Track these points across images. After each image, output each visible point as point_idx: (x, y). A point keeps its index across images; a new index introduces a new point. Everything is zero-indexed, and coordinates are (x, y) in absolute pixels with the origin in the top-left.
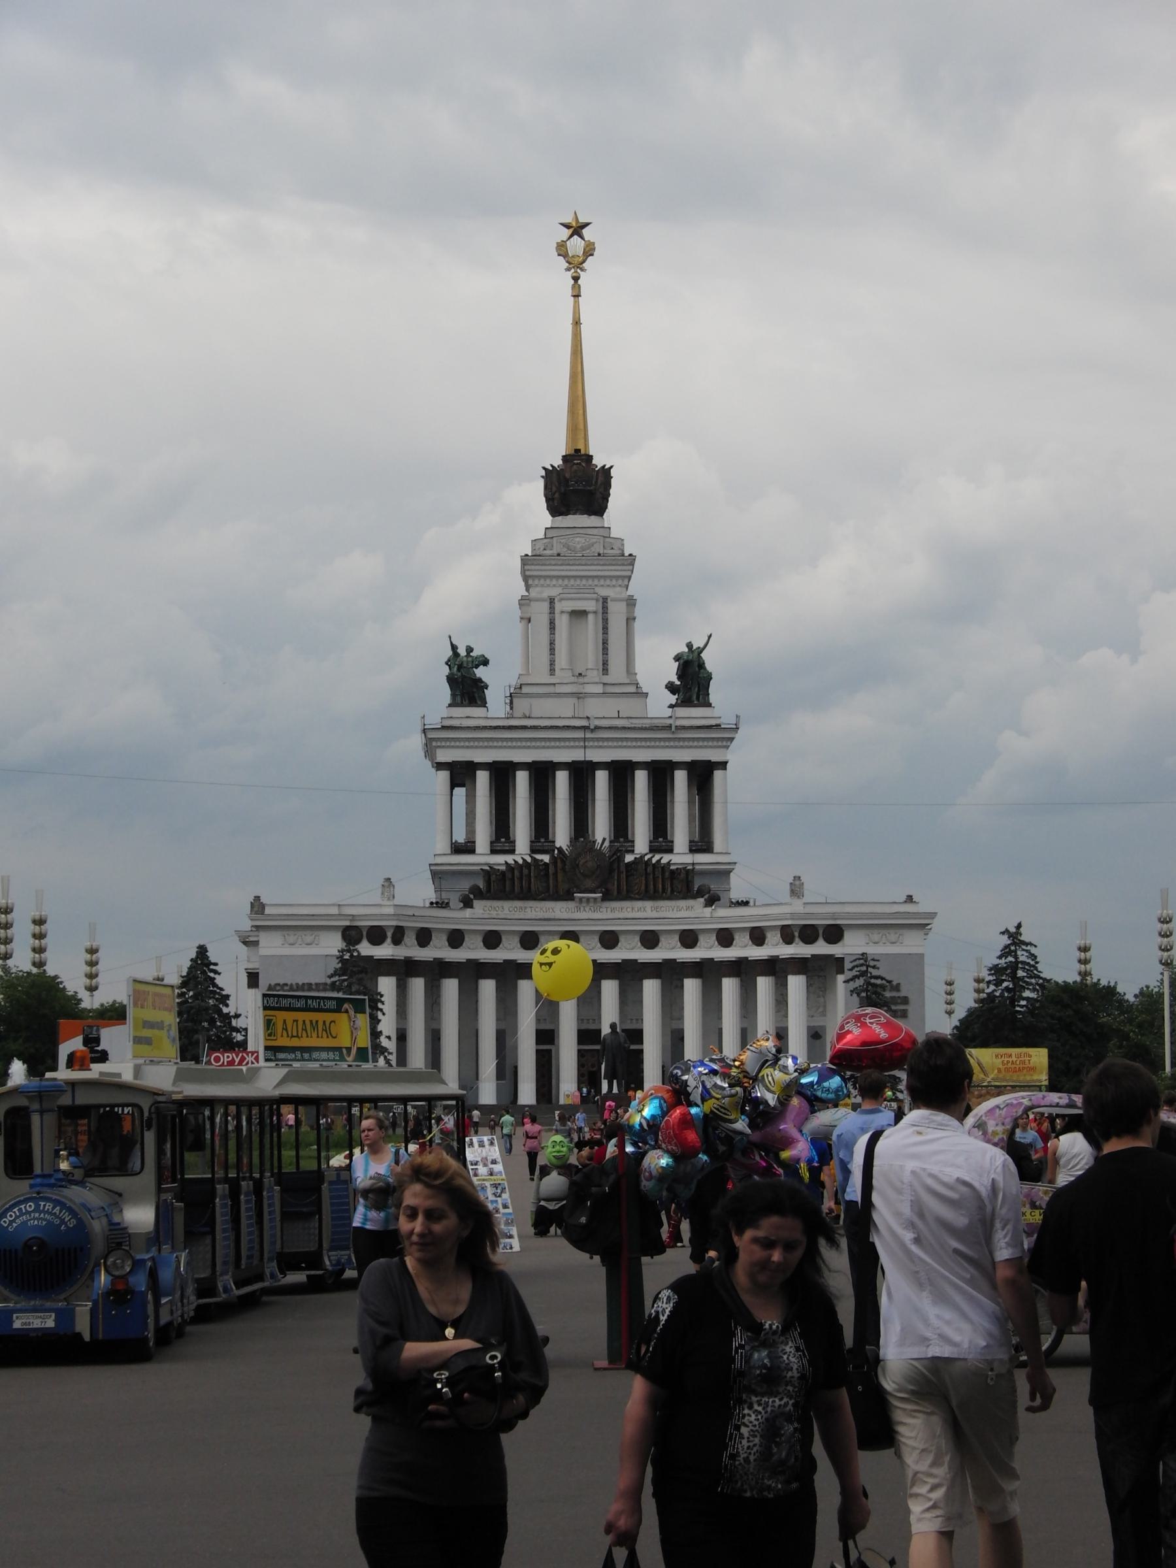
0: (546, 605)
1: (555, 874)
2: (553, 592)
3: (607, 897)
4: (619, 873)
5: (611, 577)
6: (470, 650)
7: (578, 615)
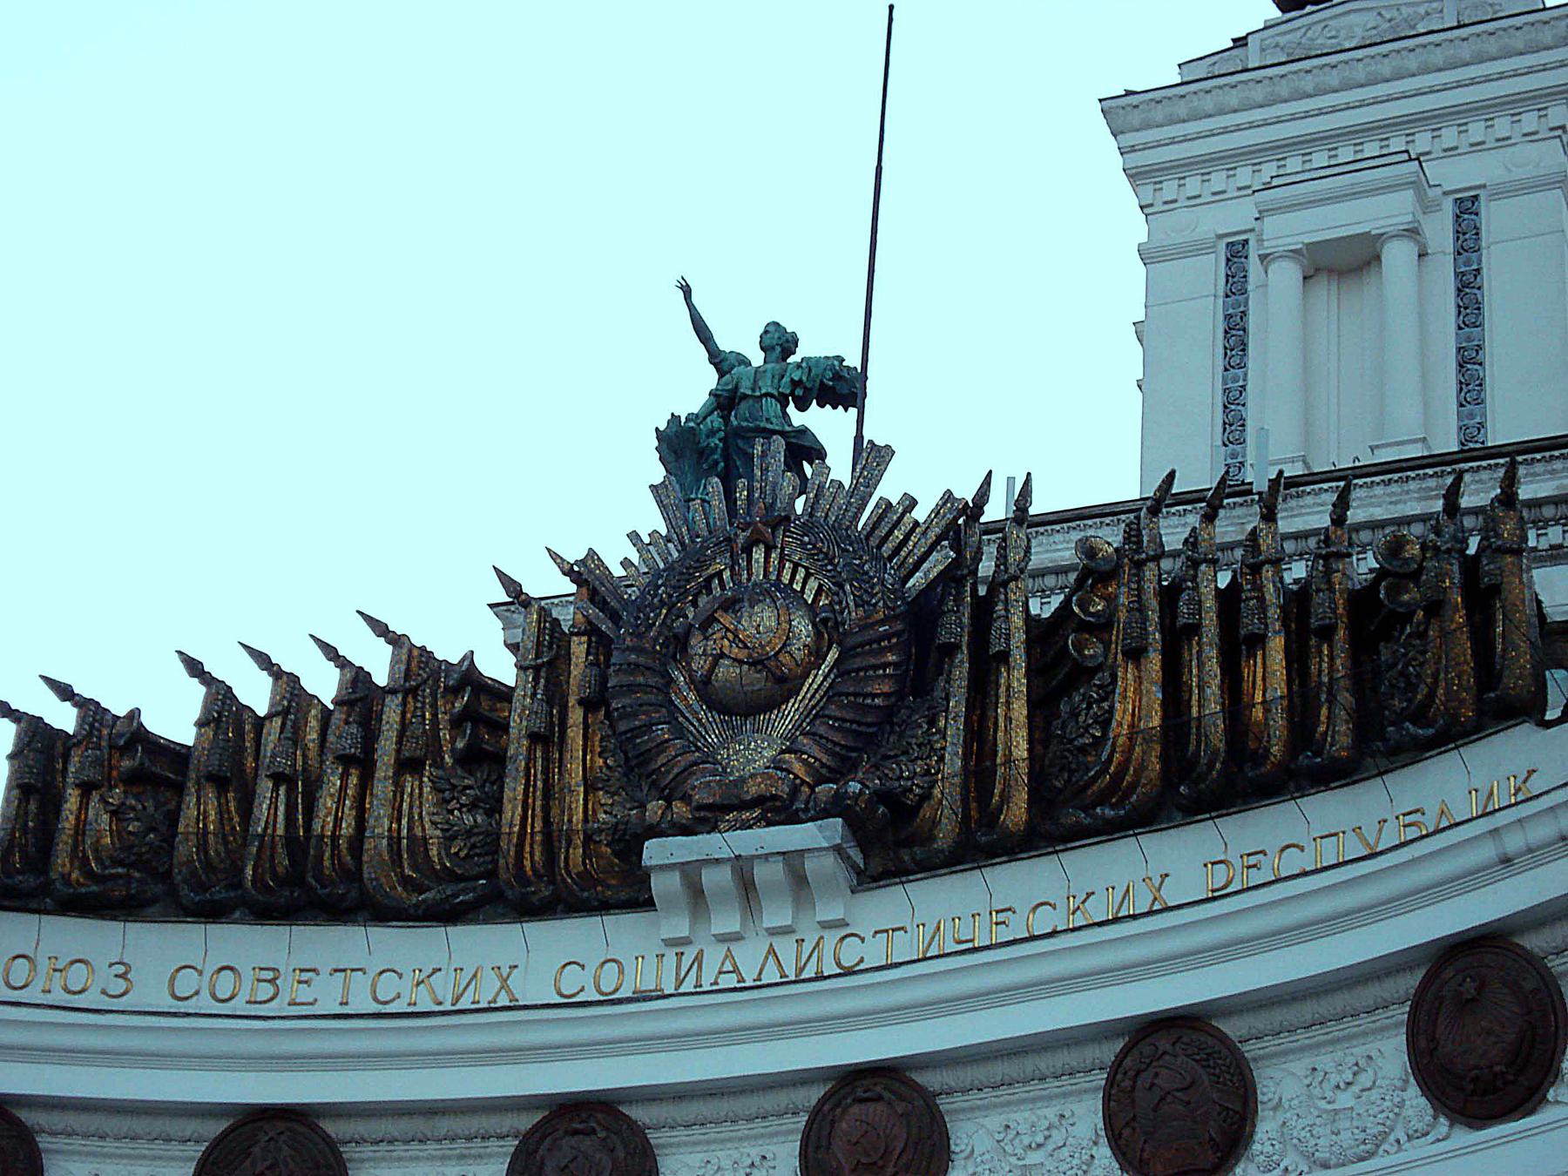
0: (1212, 268)
1: (547, 739)
2: (1236, 216)
3: (892, 846)
4: (987, 666)
5: (1486, 110)
6: (779, 342)
7: (1344, 264)
